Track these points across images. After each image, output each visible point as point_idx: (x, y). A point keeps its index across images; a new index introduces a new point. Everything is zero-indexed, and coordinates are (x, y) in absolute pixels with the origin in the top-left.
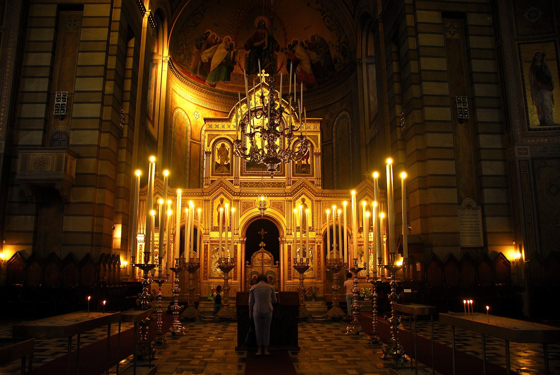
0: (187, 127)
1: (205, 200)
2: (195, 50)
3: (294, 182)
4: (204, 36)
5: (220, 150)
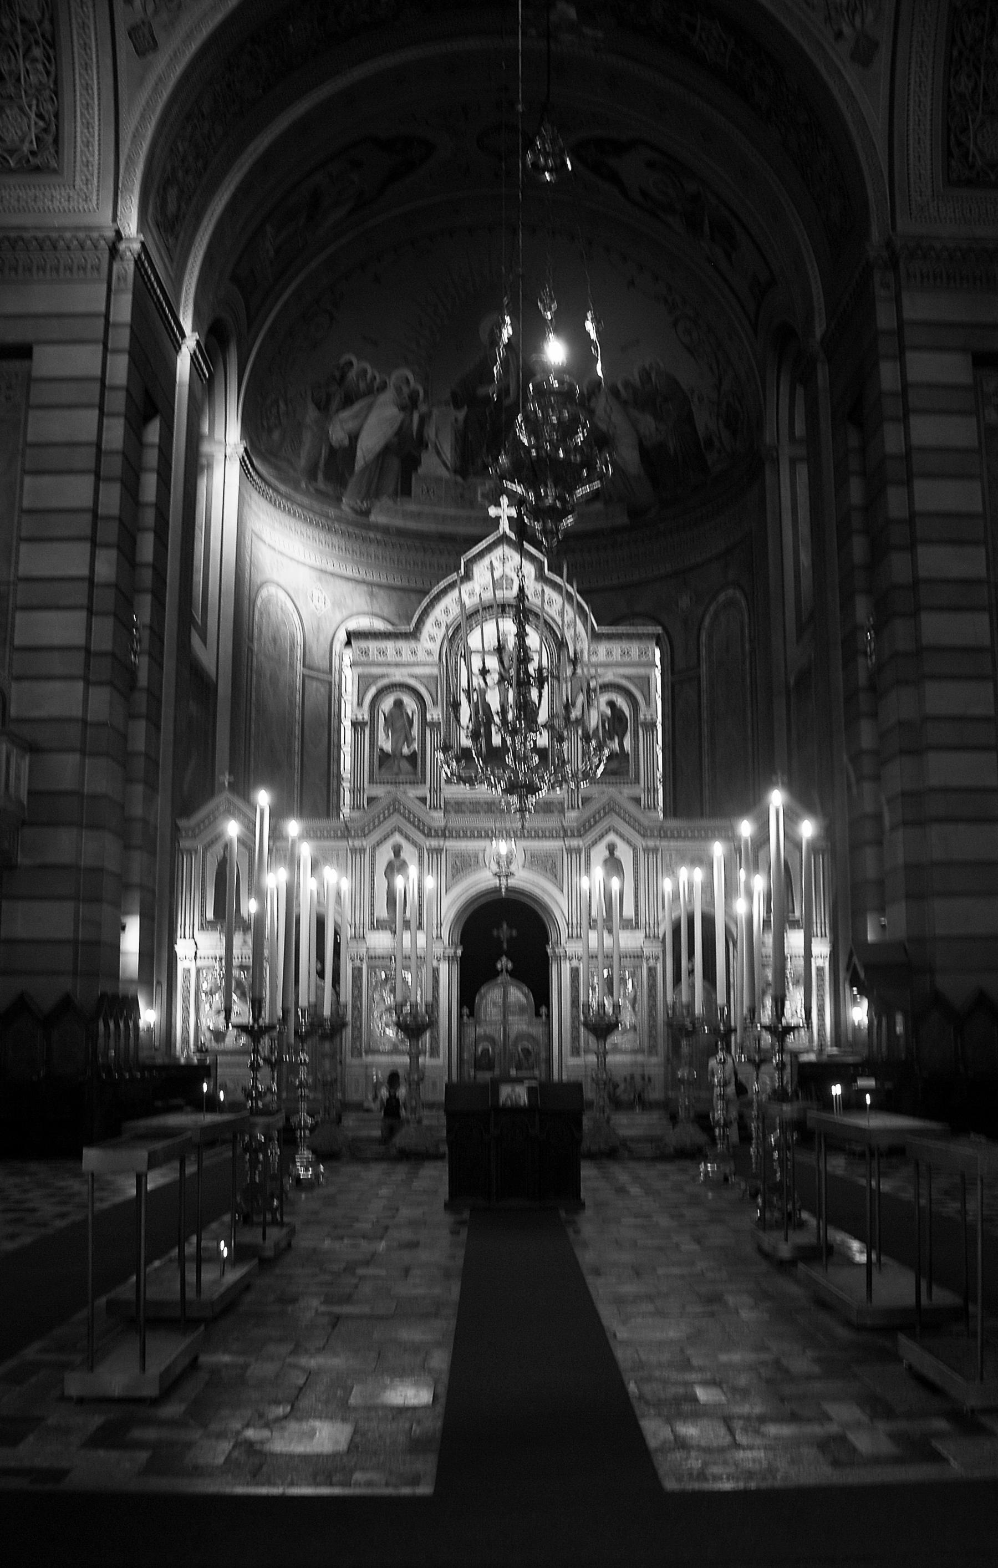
0: (293, 637)
1: (354, 851)
2: (312, 414)
3: (586, 800)
4: (337, 374)
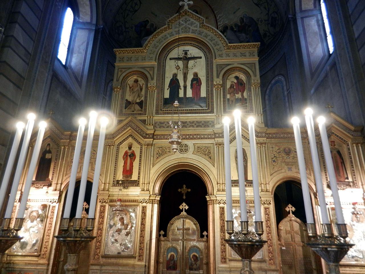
5: (133, 86)
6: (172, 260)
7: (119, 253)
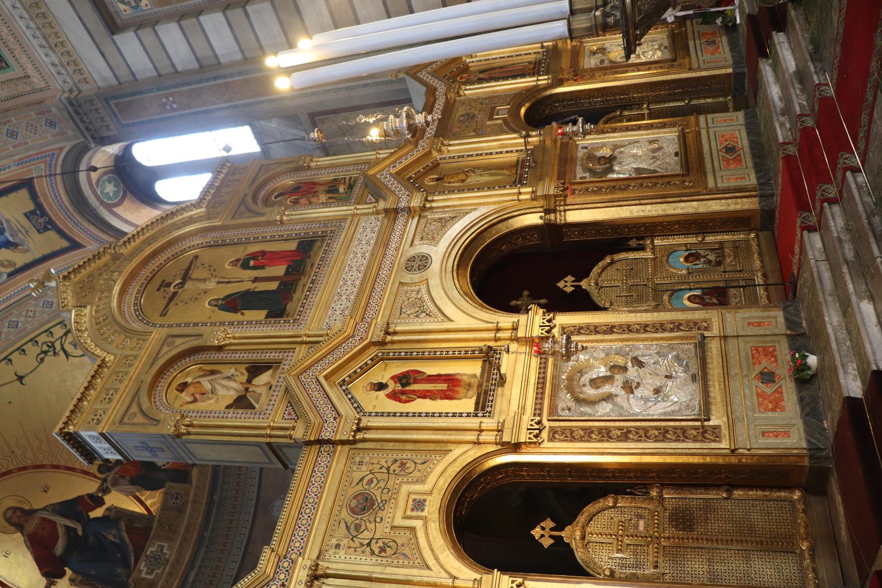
5: (193, 394)
6: (703, 299)
7: (694, 378)
